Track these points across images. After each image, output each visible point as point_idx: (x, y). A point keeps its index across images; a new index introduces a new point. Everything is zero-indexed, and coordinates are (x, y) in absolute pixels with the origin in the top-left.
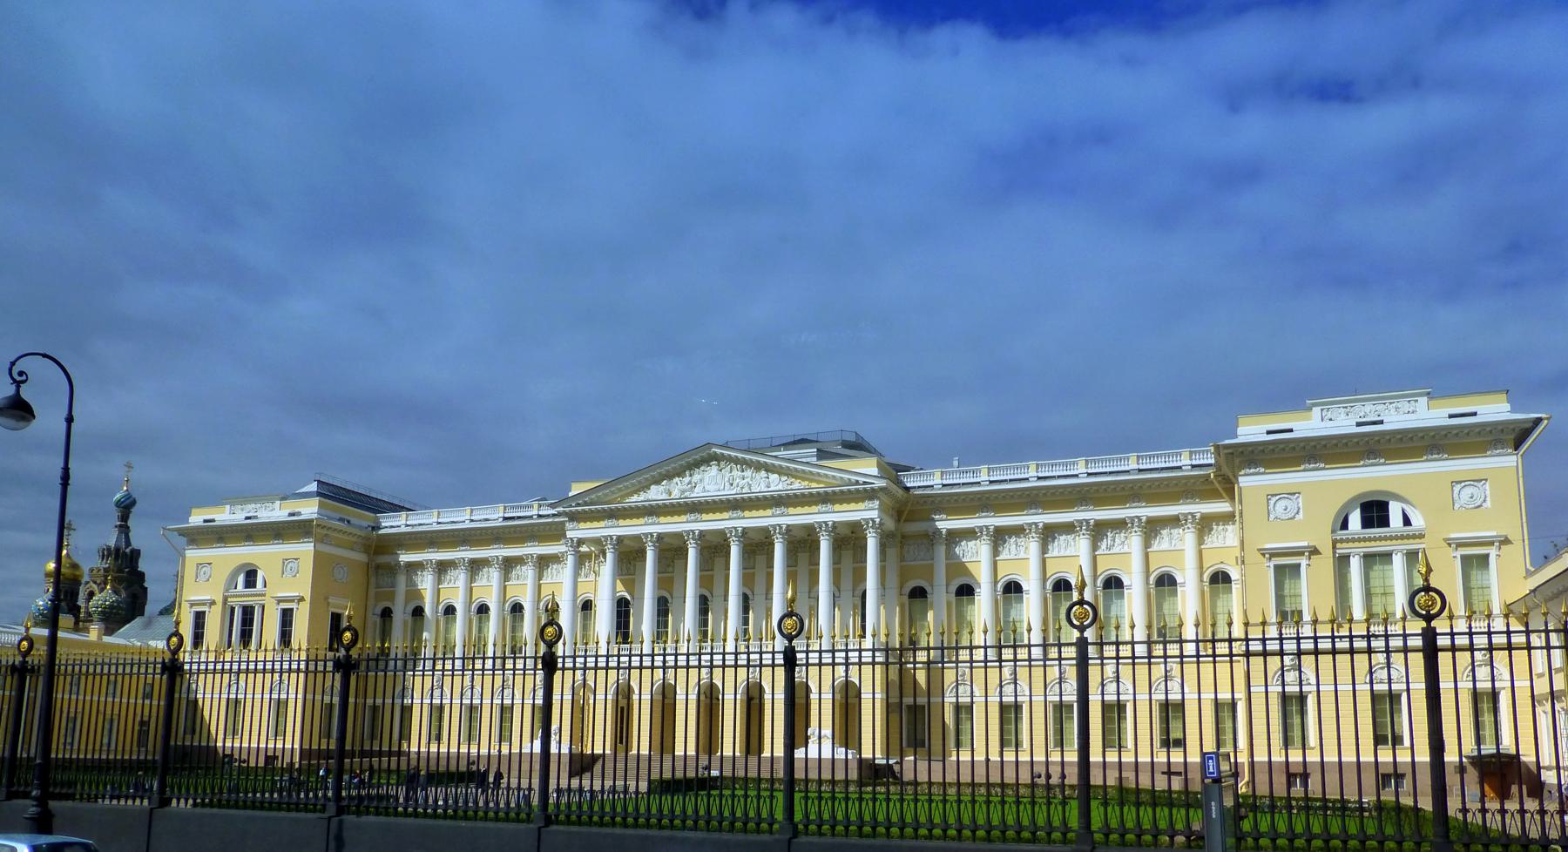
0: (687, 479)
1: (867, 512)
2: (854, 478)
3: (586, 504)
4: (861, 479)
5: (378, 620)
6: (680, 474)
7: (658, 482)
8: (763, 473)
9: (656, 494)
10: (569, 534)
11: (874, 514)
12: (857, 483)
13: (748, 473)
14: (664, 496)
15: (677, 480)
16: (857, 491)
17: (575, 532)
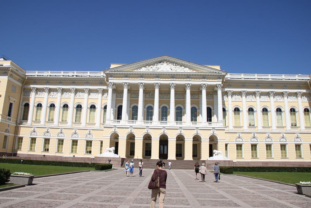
0: (155, 66)
1: (219, 82)
2: (215, 71)
3: (118, 71)
4: (217, 72)
5: (23, 107)
6: (153, 64)
7: (145, 67)
8: (183, 67)
9: (143, 70)
10: (110, 81)
11: (221, 83)
12: (216, 73)
13: (178, 67)
14: (147, 71)
15: (152, 66)
16: (216, 75)
17: (112, 80)
